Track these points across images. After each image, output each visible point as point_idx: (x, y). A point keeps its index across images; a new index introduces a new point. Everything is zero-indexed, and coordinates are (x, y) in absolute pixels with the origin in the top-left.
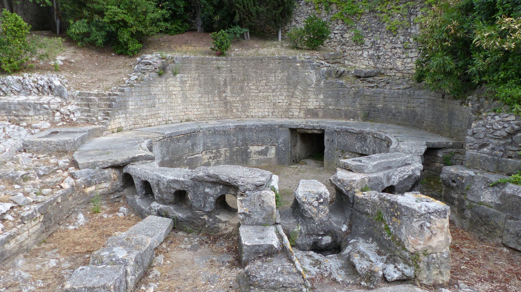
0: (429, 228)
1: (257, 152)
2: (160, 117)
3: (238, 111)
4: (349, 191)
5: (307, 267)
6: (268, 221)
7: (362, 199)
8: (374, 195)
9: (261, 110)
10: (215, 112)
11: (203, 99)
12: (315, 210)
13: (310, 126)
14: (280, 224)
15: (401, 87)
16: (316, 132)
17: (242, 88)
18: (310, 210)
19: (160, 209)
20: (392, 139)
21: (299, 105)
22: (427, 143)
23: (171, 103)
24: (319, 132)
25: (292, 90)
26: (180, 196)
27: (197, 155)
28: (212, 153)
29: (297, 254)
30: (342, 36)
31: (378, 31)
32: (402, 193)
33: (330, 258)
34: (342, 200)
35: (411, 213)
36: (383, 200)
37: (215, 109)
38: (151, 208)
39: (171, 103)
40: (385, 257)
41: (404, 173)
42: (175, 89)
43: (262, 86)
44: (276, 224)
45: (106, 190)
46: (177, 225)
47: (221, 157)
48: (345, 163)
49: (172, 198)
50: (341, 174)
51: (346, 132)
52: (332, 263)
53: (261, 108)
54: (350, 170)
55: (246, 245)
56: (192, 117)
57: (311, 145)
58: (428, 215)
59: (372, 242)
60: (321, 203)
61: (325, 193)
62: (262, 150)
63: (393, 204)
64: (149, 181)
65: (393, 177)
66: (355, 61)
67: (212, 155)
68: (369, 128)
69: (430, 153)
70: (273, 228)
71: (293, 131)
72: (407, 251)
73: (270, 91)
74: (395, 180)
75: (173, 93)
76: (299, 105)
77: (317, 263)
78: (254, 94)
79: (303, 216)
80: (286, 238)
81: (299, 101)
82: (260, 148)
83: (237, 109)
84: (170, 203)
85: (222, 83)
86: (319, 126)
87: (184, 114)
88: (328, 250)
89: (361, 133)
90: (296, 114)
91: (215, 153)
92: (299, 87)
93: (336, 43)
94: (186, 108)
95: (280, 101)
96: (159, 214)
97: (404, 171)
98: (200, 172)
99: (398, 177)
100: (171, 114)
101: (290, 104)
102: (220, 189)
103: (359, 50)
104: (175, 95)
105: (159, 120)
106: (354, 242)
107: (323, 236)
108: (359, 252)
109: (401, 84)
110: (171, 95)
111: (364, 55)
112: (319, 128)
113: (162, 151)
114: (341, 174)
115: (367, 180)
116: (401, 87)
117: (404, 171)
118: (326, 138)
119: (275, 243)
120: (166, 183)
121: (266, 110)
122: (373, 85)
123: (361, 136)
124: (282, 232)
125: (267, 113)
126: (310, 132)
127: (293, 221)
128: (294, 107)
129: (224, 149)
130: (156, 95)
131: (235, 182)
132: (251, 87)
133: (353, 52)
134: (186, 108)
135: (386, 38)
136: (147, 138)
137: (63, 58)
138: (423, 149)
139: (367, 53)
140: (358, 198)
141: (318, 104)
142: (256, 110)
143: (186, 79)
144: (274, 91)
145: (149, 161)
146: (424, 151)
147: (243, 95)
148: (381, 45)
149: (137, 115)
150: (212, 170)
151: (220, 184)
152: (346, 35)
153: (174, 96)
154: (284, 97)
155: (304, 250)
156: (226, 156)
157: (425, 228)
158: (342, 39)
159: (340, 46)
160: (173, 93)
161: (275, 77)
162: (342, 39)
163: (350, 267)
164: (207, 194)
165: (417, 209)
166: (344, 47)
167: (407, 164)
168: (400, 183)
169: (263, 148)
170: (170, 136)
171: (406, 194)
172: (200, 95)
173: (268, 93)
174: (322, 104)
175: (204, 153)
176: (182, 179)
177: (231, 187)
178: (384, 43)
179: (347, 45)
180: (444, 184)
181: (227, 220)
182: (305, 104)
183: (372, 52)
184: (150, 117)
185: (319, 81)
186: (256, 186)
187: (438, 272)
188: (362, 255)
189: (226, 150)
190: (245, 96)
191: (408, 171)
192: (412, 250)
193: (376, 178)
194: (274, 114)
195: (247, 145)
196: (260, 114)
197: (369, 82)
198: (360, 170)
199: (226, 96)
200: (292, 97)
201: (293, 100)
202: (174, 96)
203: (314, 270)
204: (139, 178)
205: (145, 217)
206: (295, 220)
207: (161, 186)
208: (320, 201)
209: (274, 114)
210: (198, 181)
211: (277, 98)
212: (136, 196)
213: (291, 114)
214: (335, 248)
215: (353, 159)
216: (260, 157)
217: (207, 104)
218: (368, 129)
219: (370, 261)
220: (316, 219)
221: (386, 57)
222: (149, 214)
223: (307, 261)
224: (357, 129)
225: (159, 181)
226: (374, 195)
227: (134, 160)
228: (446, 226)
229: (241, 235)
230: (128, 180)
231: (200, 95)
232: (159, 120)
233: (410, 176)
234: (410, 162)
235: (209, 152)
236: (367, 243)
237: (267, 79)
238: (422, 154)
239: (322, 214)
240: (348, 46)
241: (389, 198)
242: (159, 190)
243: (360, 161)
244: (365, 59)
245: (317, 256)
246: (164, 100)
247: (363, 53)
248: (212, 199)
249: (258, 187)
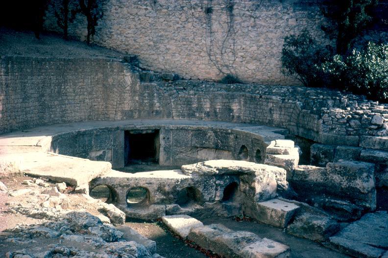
3: (56, 117)
13: (145, 127)
16: (150, 132)
30: (135, 40)
71: (127, 133)
95: (96, 104)
142: (73, 115)
158: (135, 44)
185: (133, 84)
213: (108, 116)
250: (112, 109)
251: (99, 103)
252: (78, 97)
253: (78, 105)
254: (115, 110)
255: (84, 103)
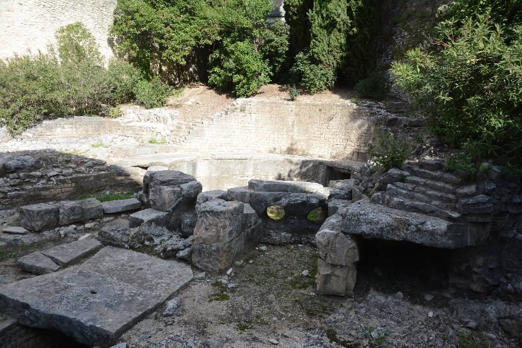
17: (307, 130)
41: (298, 198)
42: (249, 125)
75: (248, 128)
85: (291, 124)
97: (298, 196)
99: (287, 201)
113: (209, 168)
117: (298, 196)
137: (193, 100)
160: (248, 128)
201: (349, 143)
202: (248, 131)
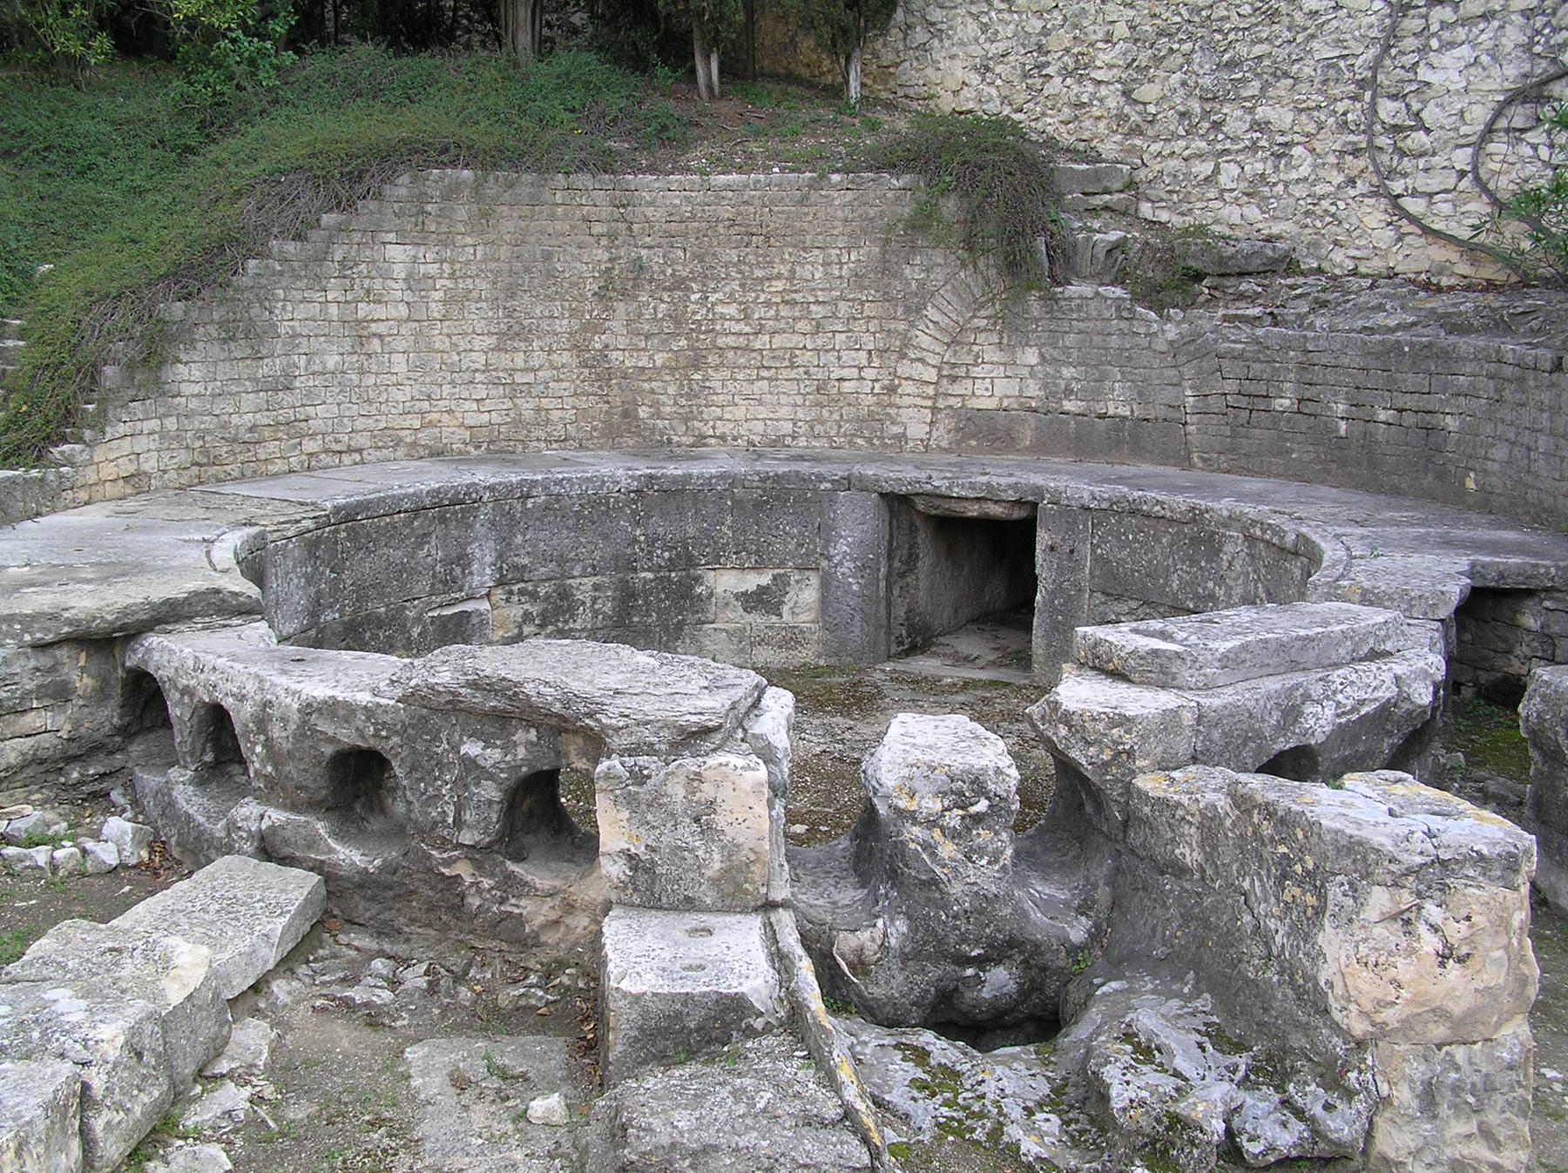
0: (1435, 929)
1: (737, 596)
2: (313, 436)
3: (658, 415)
4: (1106, 764)
5: (898, 1096)
6: (738, 894)
7: (1163, 803)
8: (1206, 789)
9: (763, 413)
10: (555, 416)
11: (504, 360)
12: (947, 850)
13: (972, 486)
14: (785, 904)
15: (1380, 319)
16: (996, 510)
18: (926, 846)
19: (272, 828)
20: (1323, 544)
21: (931, 390)
22: (1473, 565)
23: (362, 372)
24: (1018, 514)
25: (902, 326)
26: (356, 778)
27: (468, 607)
28: (534, 596)
29: (845, 1039)
30: (1126, 93)
31: (1286, 75)
32: (1333, 778)
33: (1006, 1062)
34: (1072, 808)
35: (1360, 860)
36: (1242, 802)
37: (556, 403)
38: (232, 827)
39: (362, 372)
40: (1242, 1061)
42: (380, 312)
43: (768, 304)
44: (769, 906)
45: (46, 740)
46: (340, 900)
47: (573, 617)
48: (1098, 643)
49: (317, 782)
50: (1079, 692)
51: (1132, 513)
52: (1009, 1077)
53: (761, 402)
54: (1118, 675)
55: (625, 995)
56: (453, 435)
57: (977, 575)
58: (1439, 874)
59: (1197, 993)
60: (978, 819)
61: (998, 771)
62: (762, 590)
63: (1285, 822)
64: (228, 703)
65: (1309, 709)
66: (1185, 207)
67: (534, 609)
68: (1233, 500)
69: (1483, 610)
70: (754, 924)
71: (897, 503)
72: (1336, 1028)
73: (802, 326)
74: (1319, 722)
75: (374, 327)
76: (931, 390)
77: (941, 1081)
78: (731, 341)
79: (894, 876)
80: (805, 969)
81: (931, 375)
82: (753, 581)
83: (655, 404)
84: (312, 806)
85: (592, 286)
86: (1015, 487)
87: (417, 424)
88: (1006, 1028)
89: (1196, 516)
90: (917, 430)
91: (548, 597)
92: (930, 312)
93: (1102, 125)
94: (429, 398)
95: (845, 373)
96: (269, 849)
98: (444, 669)
99: (1329, 712)
100: (360, 423)
101: (892, 390)
102: (529, 744)
103: (1200, 156)
104: (381, 337)
105: (310, 446)
106: (1116, 991)
107: (981, 962)
108: (1128, 1037)
109: (1380, 308)
110: (361, 340)
111: (1223, 180)
112: (1011, 496)
114: (1079, 692)
115: (1188, 718)
116: (1380, 319)
118: (1043, 538)
119: (753, 980)
120: (296, 717)
121: (785, 412)
122: (1256, 311)
123: (1201, 538)
124: (790, 940)
125: (787, 427)
126: (973, 511)
127: (849, 895)
128: (907, 401)
129: (589, 582)
130: (295, 336)
131: (590, 715)
132: (719, 309)
133: (1173, 164)
134: (429, 398)
135: (1319, 107)
136: (249, 523)
138: (1455, 591)
139: (1234, 170)
140: (1143, 796)
141: (1012, 387)
142: (740, 413)
143: (433, 269)
144: (818, 329)
145: (235, 621)
146: (1455, 600)
147: (683, 343)
148: (1297, 138)
149: (209, 422)
150: (493, 661)
151: (530, 724)
152: (1148, 92)
153: (376, 344)
154: (863, 354)
155: (891, 1023)
156: (596, 613)
157: (1422, 929)
158: (1127, 109)
159: (1118, 137)
160: (374, 327)
161: (826, 264)
162: (1127, 109)
163: (1083, 1101)
164: (470, 764)
165: (1389, 846)
166: (1138, 142)
167: (1374, 655)
168: (1343, 733)
169: (765, 579)
170: (347, 515)
171: (1352, 780)
172: (492, 340)
173: (796, 338)
174: (1033, 389)
175: (499, 594)
176: (364, 698)
177: (571, 728)
178: (1312, 128)
179: (1150, 133)
180: (1535, 745)
181: (558, 883)
182: (957, 389)
183: (1259, 167)
184: (267, 433)
186: (682, 729)
187: (1472, 1127)
188: (1146, 1052)
189: (596, 587)
190: (691, 348)
191: (1370, 686)
192: (1359, 1028)
193: (1232, 711)
194: (818, 428)
195: (691, 563)
196: (759, 427)
197: (1241, 297)
198: (1155, 671)
199: (606, 346)
200: (903, 356)
201: (904, 369)
202: (376, 344)
203: (927, 1112)
204: (187, 691)
205: (210, 861)
206: (860, 894)
207: (276, 731)
208: (973, 810)
209: (818, 428)
210: (432, 712)
211: (832, 357)
212: (174, 773)
213: (896, 430)
214: (1037, 1019)
215: (1134, 625)
216: (749, 618)
217: (519, 378)
218: (1224, 506)
219: (1177, 1074)
220: (956, 889)
221: (1320, 190)
222: (228, 849)
223: (902, 1070)
224: (1180, 502)
225: (267, 704)
226: (1206, 789)
227: (169, 615)
228: (1516, 923)
229: (609, 949)
230: (144, 698)
231: (492, 340)
232: (310, 446)
233: (1385, 710)
234: (1389, 646)
235: (522, 592)
236: (1171, 995)
237: (792, 276)
238: (1446, 611)
239: (979, 873)
240: (1156, 138)
241: (1272, 796)
242: (269, 744)
243: (1164, 635)
244: (1227, 196)
245: (942, 1050)
246: (332, 361)
247: (1217, 170)
248: (489, 791)
249: (693, 737)
250: (919, 401)
251: (861, 369)
252: (767, 338)
253: (764, 373)
254: (929, 403)
255: (792, 366)
